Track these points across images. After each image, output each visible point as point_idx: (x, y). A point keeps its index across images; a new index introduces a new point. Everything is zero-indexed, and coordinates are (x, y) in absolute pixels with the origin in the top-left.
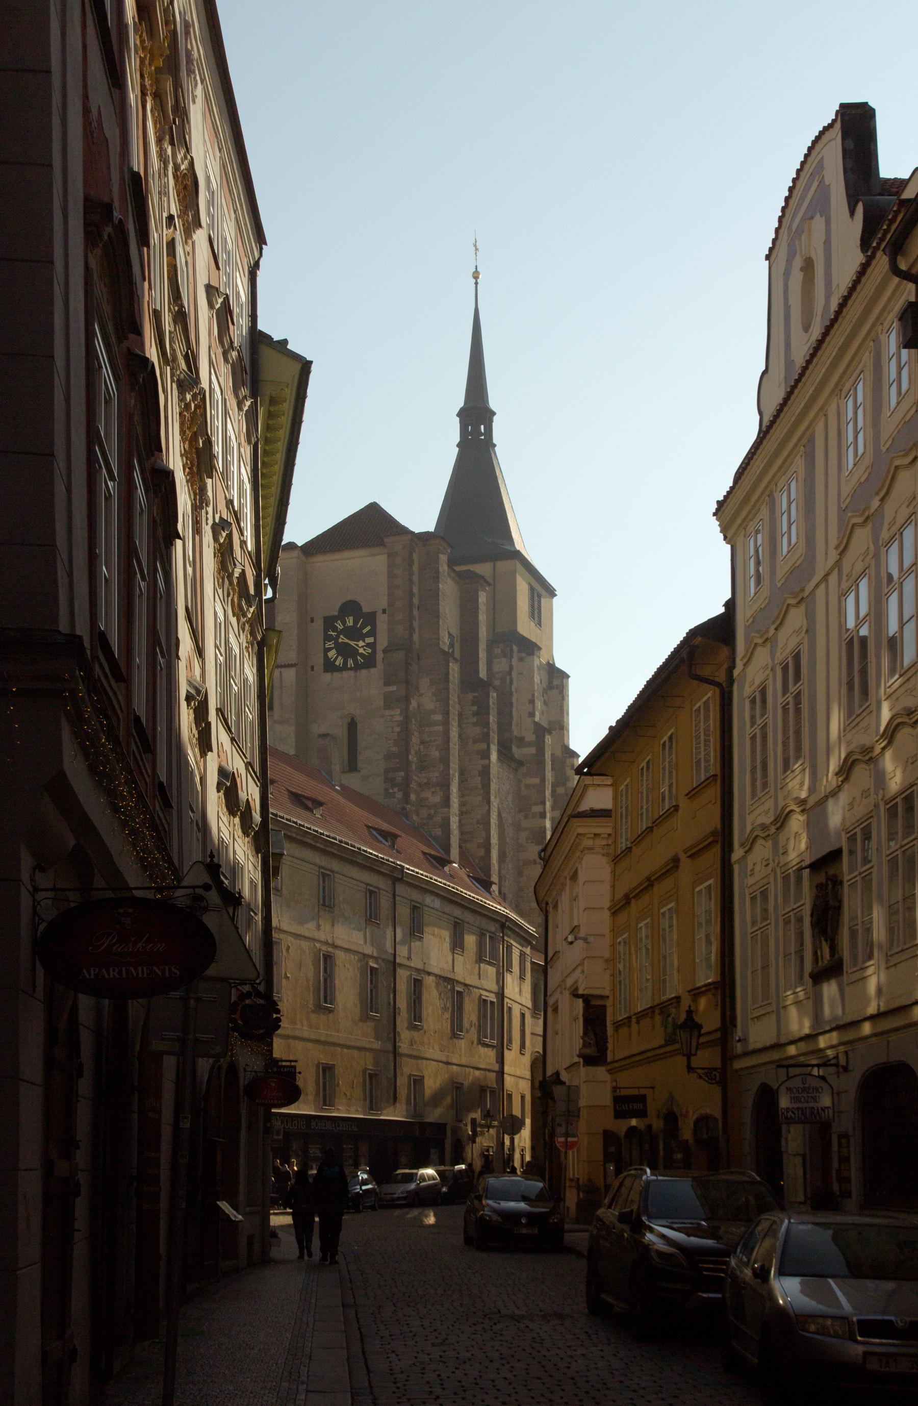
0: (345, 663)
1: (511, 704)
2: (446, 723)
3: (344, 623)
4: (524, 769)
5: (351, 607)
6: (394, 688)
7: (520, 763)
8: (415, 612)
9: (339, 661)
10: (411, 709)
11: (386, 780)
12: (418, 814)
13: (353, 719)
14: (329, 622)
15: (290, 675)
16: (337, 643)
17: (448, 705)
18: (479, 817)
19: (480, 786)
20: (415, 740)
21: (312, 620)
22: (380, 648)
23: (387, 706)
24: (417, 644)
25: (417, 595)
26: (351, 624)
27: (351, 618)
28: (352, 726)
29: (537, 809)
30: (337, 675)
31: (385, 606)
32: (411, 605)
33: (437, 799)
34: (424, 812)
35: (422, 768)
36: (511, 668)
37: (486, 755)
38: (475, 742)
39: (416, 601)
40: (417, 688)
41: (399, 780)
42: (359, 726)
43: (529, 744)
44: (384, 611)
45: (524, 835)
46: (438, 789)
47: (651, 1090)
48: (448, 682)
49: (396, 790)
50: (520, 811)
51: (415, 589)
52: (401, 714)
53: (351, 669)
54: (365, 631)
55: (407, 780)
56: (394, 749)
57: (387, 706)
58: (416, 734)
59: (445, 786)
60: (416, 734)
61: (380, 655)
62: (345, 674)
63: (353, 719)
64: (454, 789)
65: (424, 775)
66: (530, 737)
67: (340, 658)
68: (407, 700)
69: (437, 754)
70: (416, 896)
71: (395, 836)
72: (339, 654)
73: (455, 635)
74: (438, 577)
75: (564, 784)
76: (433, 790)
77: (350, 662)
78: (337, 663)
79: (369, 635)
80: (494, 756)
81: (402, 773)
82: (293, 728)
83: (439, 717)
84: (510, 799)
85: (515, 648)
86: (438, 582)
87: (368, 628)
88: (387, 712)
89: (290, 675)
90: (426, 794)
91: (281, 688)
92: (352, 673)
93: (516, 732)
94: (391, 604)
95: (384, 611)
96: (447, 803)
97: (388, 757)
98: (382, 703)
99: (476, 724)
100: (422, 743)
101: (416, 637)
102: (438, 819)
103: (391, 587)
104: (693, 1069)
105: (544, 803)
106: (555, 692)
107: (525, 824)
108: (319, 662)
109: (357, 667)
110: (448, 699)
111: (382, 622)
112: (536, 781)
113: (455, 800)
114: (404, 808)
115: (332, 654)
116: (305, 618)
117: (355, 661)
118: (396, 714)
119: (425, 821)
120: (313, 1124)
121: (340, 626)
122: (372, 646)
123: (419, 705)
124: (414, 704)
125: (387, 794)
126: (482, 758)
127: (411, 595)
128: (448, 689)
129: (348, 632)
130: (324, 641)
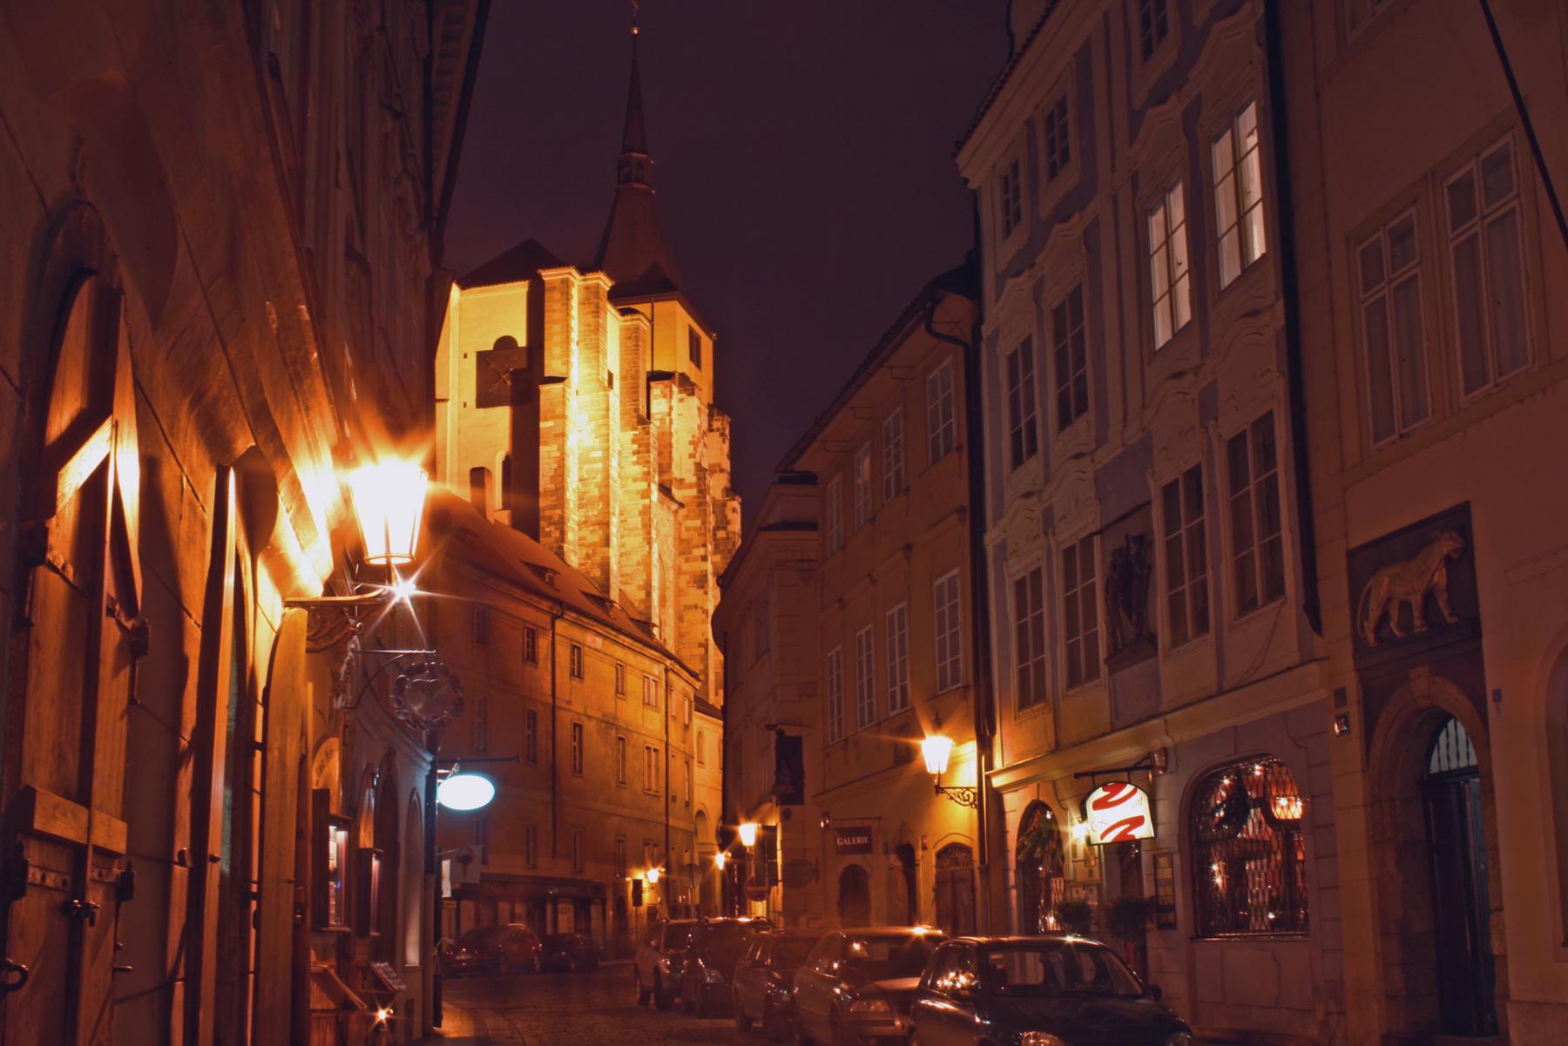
1: (671, 445)
4: (683, 512)
7: (682, 505)
29: (700, 552)
33: (596, 538)
36: (671, 408)
37: (646, 494)
38: (635, 480)
43: (690, 486)
45: (684, 579)
50: (681, 553)
56: (551, 486)
66: (691, 478)
70: (576, 633)
75: (725, 528)
81: (559, 511)
84: (671, 540)
85: (675, 389)
90: (585, 532)
93: (676, 472)
96: (606, 542)
99: (637, 463)
100: (581, 480)
102: (597, 559)
105: (704, 546)
106: (716, 434)
107: (685, 567)
112: (698, 523)
113: (614, 540)
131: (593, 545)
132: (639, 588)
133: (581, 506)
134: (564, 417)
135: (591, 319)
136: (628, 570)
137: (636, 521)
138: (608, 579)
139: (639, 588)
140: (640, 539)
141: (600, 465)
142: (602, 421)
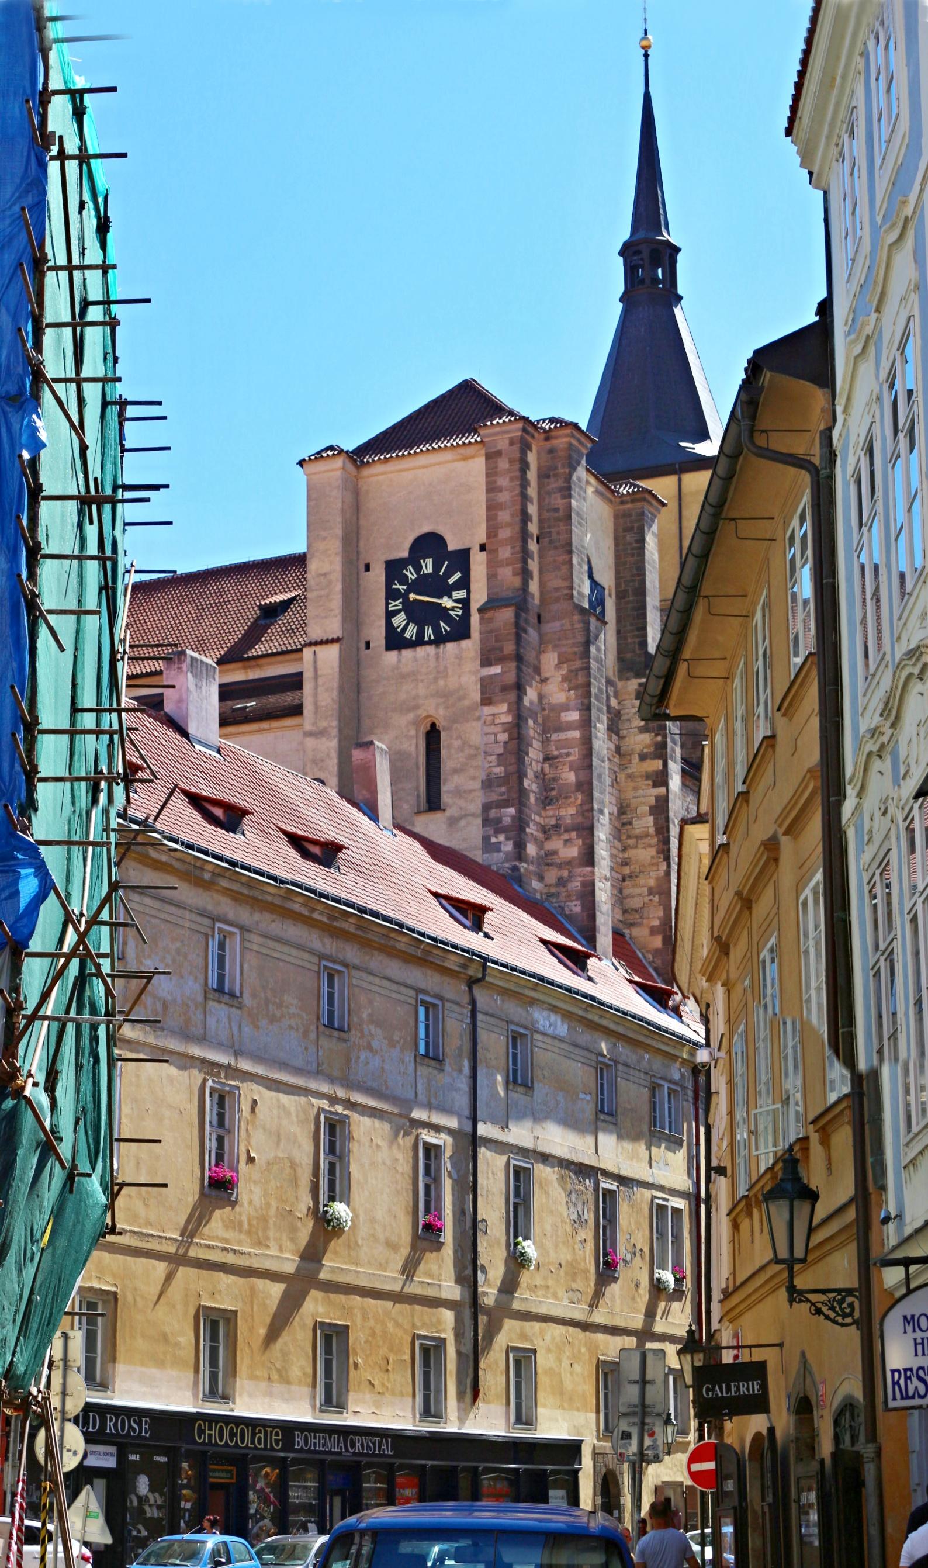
0: (420, 633)
2: (586, 724)
3: (418, 568)
5: (429, 544)
6: (497, 670)
8: (533, 546)
9: (411, 632)
10: (526, 702)
11: (486, 822)
12: (541, 878)
13: (433, 725)
14: (394, 569)
15: (330, 655)
16: (406, 603)
17: (588, 694)
18: (652, 883)
19: (652, 830)
20: (534, 753)
21: (367, 568)
22: (475, 606)
23: (486, 701)
24: (537, 595)
25: (535, 519)
26: (430, 570)
27: (429, 561)
28: (433, 736)
30: (407, 653)
31: (484, 540)
32: (525, 535)
33: (573, 852)
34: (552, 876)
35: (546, 801)
37: (661, 779)
38: (643, 757)
39: (533, 528)
40: (537, 670)
41: (507, 821)
42: (443, 735)
44: (483, 548)
46: (574, 834)
47: (777, 1348)
48: (589, 657)
49: (501, 838)
51: (532, 509)
52: (509, 711)
53: (430, 643)
54: (451, 581)
55: (520, 823)
56: (499, 770)
57: (486, 701)
58: (536, 744)
59: (587, 830)
60: (536, 744)
61: (475, 618)
62: (421, 651)
63: (433, 725)
64: (602, 834)
65: (551, 813)
67: (412, 625)
68: (519, 688)
69: (570, 777)
70: (513, 1009)
71: (482, 910)
72: (410, 619)
73: (606, 586)
74: (569, 489)
76: (566, 836)
77: (429, 633)
78: (407, 635)
79: (458, 586)
80: (675, 781)
81: (512, 811)
82: (334, 743)
83: (574, 716)
86: (570, 496)
87: (458, 575)
88: (487, 710)
89: (330, 655)
91: (316, 677)
92: (431, 650)
94: (492, 533)
95: (483, 548)
96: (589, 858)
97: (488, 784)
98: (477, 697)
100: (547, 759)
101: (534, 587)
102: (576, 885)
103: (492, 508)
104: (801, 1293)
108: (377, 634)
109: (440, 640)
110: (588, 684)
111: (479, 563)
113: (603, 853)
114: (515, 869)
115: (399, 620)
116: (355, 566)
117: (437, 630)
118: (502, 712)
119: (553, 890)
120: (299, 1441)
121: (411, 574)
122: (465, 603)
123: (541, 697)
124: (531, 695)
125: (488, 846)
126: (655, 786)
127: (525, 518)
128: (588, 668)
129: (422, 584)
130: (387, 599)
131: (569, 863)
132: (653, 931)
133: (546, 801)
134: (519, 658)
135: (558, 501)
136: (635, 903)
137: (646, 823)
138: (593, 917)
139: (653, 931)
140: (653, 852)
141: (576, 734)
142: (578, 664)
